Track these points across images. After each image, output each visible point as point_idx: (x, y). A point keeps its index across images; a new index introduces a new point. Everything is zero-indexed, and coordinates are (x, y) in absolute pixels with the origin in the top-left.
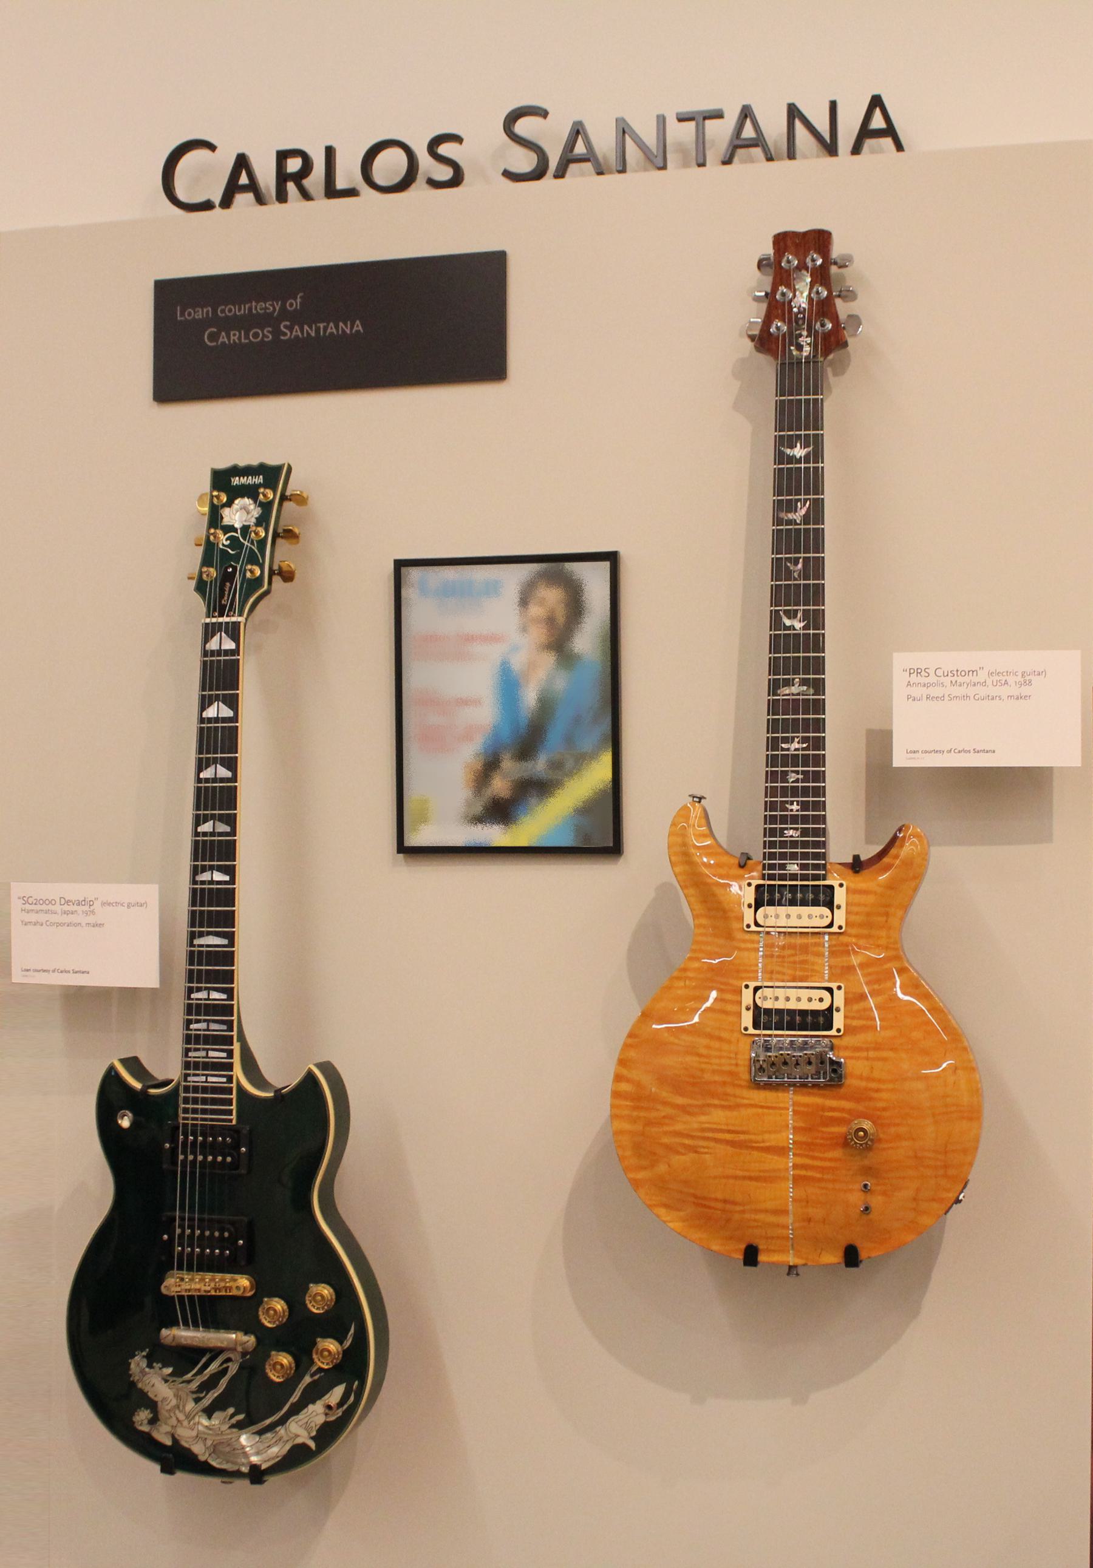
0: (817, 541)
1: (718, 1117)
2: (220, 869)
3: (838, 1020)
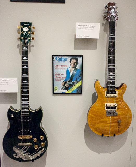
0: (114, 47)
1: (102, 120)
2: (26, 81)
3: (117, 108)
